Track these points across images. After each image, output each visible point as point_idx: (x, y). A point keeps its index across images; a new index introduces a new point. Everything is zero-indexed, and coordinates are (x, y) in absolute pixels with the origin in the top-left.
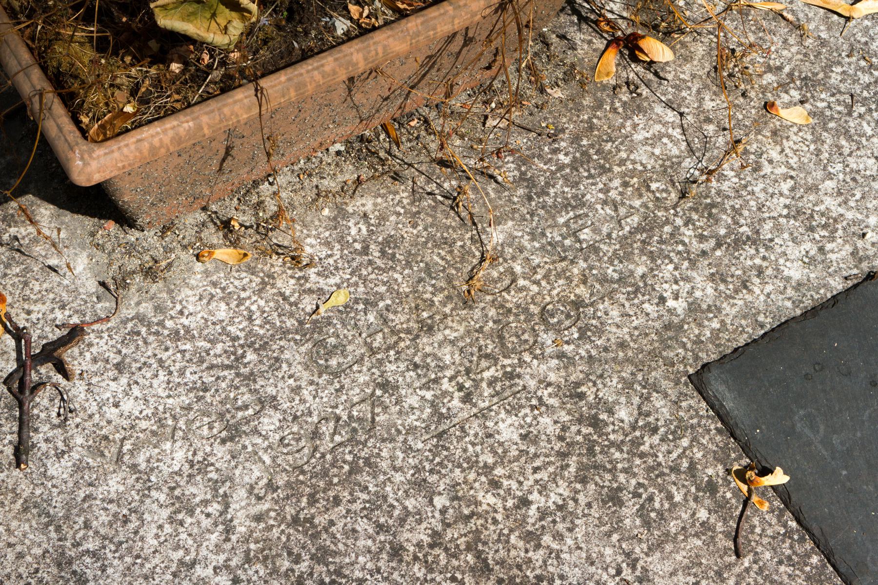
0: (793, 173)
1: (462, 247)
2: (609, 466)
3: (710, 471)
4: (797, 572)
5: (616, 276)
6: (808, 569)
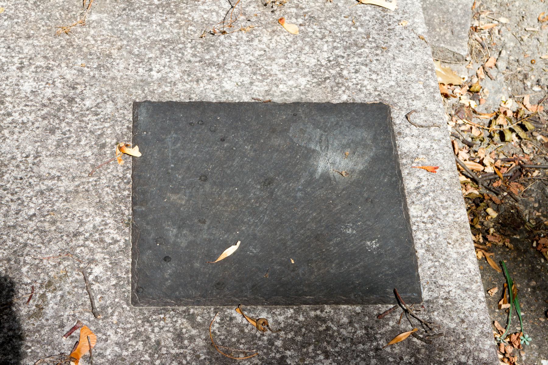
0: (267, 50)
1: (74, 15)
2: (61, 118)
3: (108, 140)
4: (113, 193)
5: (137, 53)
6: (119, 194)
